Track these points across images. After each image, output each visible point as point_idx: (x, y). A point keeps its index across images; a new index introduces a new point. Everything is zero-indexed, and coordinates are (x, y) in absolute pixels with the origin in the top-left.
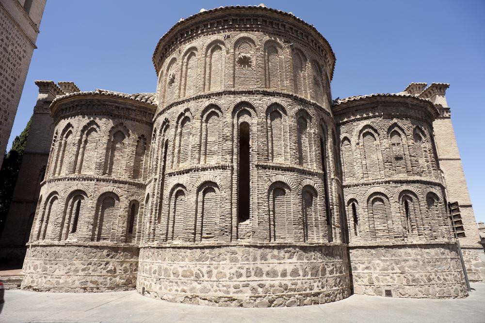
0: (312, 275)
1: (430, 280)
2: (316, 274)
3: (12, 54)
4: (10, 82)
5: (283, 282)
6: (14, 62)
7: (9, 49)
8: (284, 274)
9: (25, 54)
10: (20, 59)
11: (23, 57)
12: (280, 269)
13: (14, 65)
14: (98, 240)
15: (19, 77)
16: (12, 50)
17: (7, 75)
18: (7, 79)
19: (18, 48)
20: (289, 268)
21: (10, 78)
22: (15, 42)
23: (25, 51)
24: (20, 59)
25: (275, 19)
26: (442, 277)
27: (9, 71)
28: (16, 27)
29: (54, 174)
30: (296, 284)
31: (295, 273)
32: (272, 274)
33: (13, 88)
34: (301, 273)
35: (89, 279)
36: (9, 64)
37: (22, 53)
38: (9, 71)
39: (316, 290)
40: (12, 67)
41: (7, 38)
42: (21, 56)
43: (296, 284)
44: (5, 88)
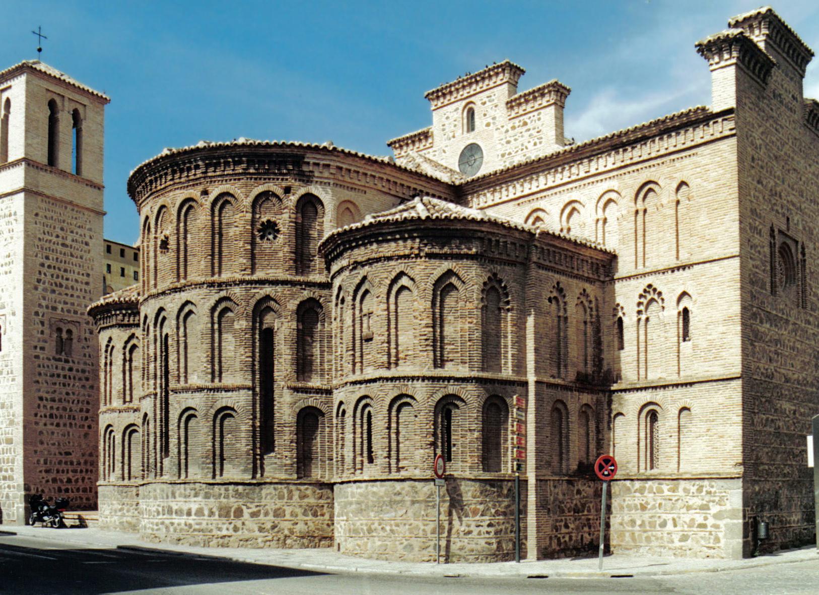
0: (220, 516)
2: (227, 515)
3: (74, 244)
6: (79, 253)
7: (69, 242)
9: (92, 233)
10: (87, 244)
11: (91, 238)
12: (185, 507)
13: (81, 258)
14: (399, 469)
15: (92, 269)
16: (73, 241)
17: (76, 276)
18: (76, 281)
19: (80, 231)
20: (194, 507)
21: (80, 278)
22: (73, 227)
23: (90, 230)
24: (87, 244)
27: (77, 269)
29: (106, 404)
31: (200, 512)
32: (179, 512)
33: (87, 288)
34: (206, 512)
35: (125, 519)
36: (74, 260)
37: (88, 233)
38: (77, 269)
39: (225, 532)
42: (87, 239)
43: (200, 524)
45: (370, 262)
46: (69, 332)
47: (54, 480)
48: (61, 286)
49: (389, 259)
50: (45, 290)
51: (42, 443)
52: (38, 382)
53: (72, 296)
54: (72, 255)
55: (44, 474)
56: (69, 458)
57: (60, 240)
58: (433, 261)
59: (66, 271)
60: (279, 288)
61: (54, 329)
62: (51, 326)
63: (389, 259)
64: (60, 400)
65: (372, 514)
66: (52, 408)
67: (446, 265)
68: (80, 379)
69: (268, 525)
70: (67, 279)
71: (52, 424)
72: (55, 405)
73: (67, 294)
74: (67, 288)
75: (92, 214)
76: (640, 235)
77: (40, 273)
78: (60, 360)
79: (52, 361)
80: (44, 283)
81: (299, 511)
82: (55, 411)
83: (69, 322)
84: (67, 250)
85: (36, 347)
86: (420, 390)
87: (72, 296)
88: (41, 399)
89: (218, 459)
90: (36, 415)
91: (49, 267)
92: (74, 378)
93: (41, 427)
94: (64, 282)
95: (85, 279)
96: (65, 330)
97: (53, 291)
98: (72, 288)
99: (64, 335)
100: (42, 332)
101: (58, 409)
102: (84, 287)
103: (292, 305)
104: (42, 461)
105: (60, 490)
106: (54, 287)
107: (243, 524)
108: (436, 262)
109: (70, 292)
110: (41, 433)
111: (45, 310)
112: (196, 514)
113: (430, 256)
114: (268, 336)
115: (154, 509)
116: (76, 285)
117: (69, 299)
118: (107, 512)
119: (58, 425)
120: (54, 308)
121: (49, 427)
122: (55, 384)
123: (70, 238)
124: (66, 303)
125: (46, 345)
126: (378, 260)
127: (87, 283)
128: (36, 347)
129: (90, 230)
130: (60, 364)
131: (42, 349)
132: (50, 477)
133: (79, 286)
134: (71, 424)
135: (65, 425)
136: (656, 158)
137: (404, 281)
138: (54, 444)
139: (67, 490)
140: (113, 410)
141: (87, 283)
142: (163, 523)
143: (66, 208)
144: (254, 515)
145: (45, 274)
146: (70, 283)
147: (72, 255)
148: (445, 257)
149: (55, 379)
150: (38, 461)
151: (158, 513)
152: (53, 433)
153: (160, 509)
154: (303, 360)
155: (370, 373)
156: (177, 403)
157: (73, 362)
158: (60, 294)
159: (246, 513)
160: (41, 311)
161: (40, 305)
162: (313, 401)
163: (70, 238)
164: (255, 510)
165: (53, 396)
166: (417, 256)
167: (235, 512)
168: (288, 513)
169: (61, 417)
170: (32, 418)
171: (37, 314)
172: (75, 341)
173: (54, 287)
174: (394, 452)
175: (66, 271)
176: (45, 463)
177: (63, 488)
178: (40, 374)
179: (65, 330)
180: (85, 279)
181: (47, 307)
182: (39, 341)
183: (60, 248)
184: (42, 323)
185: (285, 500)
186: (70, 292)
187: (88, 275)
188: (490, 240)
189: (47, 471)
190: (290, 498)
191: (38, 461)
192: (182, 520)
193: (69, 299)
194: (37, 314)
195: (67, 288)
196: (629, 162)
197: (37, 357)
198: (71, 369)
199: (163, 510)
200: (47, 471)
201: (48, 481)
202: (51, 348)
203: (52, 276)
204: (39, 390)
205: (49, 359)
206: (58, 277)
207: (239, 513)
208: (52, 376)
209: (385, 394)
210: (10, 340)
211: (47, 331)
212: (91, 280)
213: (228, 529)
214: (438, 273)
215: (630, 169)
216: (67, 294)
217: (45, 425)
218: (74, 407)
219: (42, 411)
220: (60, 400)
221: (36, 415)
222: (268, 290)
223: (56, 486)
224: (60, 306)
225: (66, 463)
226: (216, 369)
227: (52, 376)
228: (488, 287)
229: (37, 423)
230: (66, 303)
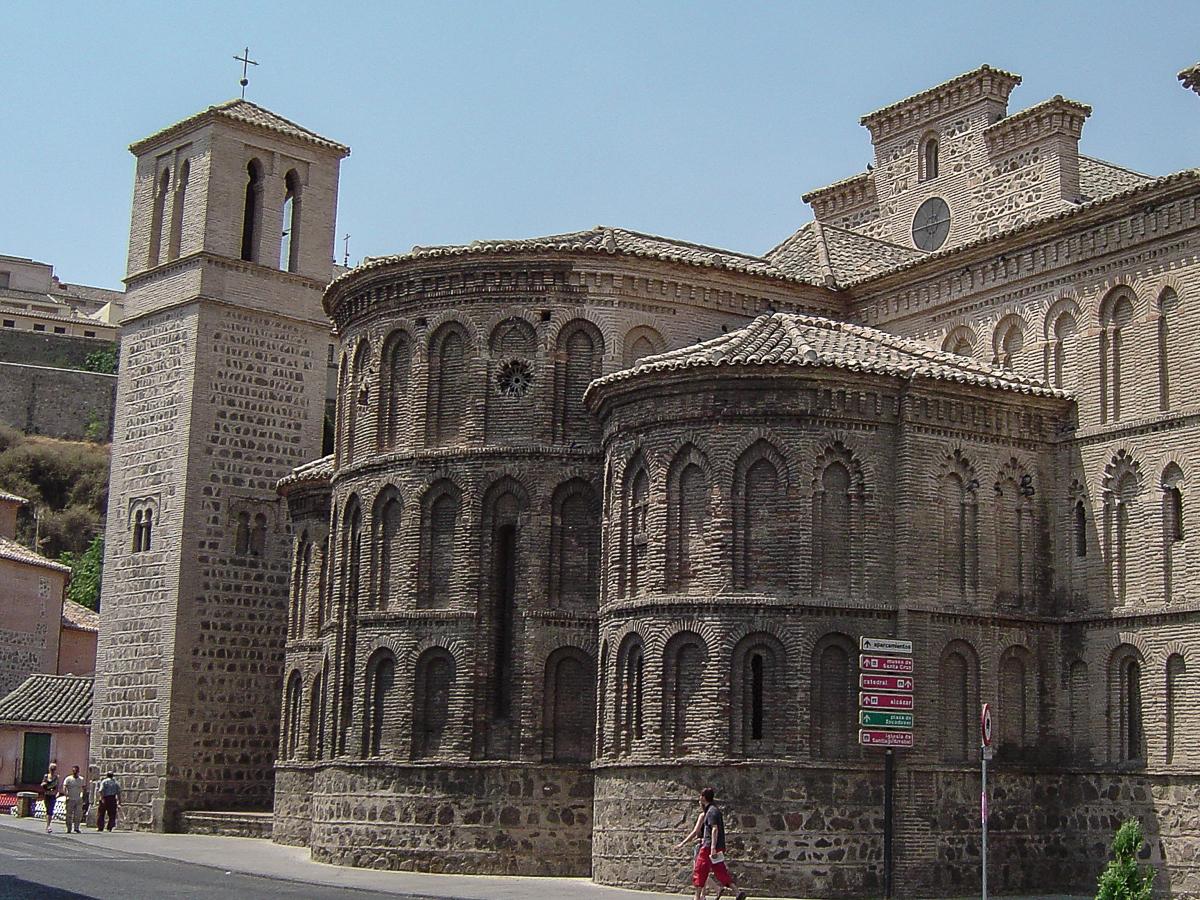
0: (418, 820)
1: (632, 848)
2: (429, 819)
4: (287, 439)
5: (372, 828)
6: (284, 393)
7: (268, 376)
8: (373, 816)
10: (299, 377)
11: (306, 367)
12: (368, 805)
16: (275, 373)
17: (277, 429)
18: (278, 437)
19: (288, 357)
20: (381, 805)
21: (284, 432)
23: (306, 354)
24: (299, 377)
25: (394, 278)
26: (656, 844)
27: (279, 418)
28: (273, 320)
30: (388, 833)
31: (388, 814)
34: (398, 814)
37: (302, 360)
38: (279, 418)
39: (422, 847)
40: (284, 405)
41: (259, 356)
42: (300, 369)
43: (388, 833)
44: (279, 455)
45: (646, 427)
46: (261, 517)
47: (219, 758)
48: (252, 445)
49: (671, 423)
50: (224, 453)
51: (202, 697)
52: (202, 599)
53: (269, 460)
54: (273, 397)
55: (201, 748)
56: (248, 721)
57: (255, 375)
58: (735, 427)
59: (260, 422)
60: (526, 465)
61: (236, 514)
62: (230, 510)
63: (671, 423)
64: (238, 628)
65: (635, 822)
66: (223, 640)
67: (755, 432)
68: (274, 593)
69: (492, 837)
70: (263, 435)
71: (221, 666)
72: (229, 635)
73: (260, 459)
74: (261, 448)
75: (311, 329)
76: (1110, 373)
77: (217, 427)
78: (242, 563)
79: (229, 566)
80: (223, 443)
81: (543, 816)
82: (227, 646)
83: (261, 502)
84: (266, 389)
85: (202, 544)
86: (710, 630)
87: (269, 460)
88: (206, 625)
89: (425, 729)
90: (196, 652)
91: (234, 417)
92: (265, 591)
93: (203, 671)
94: (257, 441)
95: (293, 432)
96: (253, 515)
97: (238, 455)
98: (270, 448)
99: (252, 523)
100: (215, 520)
101: (233, 641)
102: (290, 445)
103: (545, 490)
104: (200, 727)
105: (227, 775)
106: (239, 448)
107: (453, 834)
108: (738, 428)
109: (266, 454)
110: (202, 680)
111: (221, 485)
112: (382, 817)
113: (731, 419)
114: (507, 536)
115: (327, 807)
116: (276, 443)
117: (264, 466)
118: (283, 813)
119: (231, 668)
120: (238, 482)
121: (217, 671)
122: (231, 601)
123: (270, 370)
124: (257, 472)
125: (221, 540)
126: (655, 425)
127: (296, 440)
128: (202, 544)
129: (306, 354)
130: (242, 570)
131: (213, 546)
132: (212, 753)
133: (281, 444)
134: (254, 667)
135: (244, 668)
136: (1131, 248)
137: (694, 458)
138: (222, 699)
139: (240, 776)
140: (302, 648)
141: (296, 440)
142: (336, 831)
143: (267, 323)
144: (471, 818)
145: (225, 428)
146: (266, 441)
147: (273, 397)
148: (754, 419)
149: (230, 595)
150: (194, 727)
151: (332, 816)
152: (222, 681)
153: (334, 807)
154: (560, 573)
155: (644, 597)
156: (369, 641)
157: (265, 566)
158: (249, 459)
159: (458, 815)
160: (215, 487)
161: (214, 478)
162: (573, 637)
163: (270, 370)
164: (471, 810)
165: (225, 621)
166: (712, 420)
167: (440, 815)
168: (523, 818)
169: (238, 655)
170: (189, 657)
171: (208, 491)
172: (270, 531)
173: (239, 448)
174: (673, 728)
175: (260, 422)
176: (206, 729)
177: (234, 771)
178: (207, 586)
179: (253, 515)
180: (293, 432)
181: (226, 480)
182: (209, 534)
183: (253, 386)
184: (217, 506)
185: (521, 796)
186: (266, 454)
187: (298, 427)
188: (828, 393)
189: (207, 744)
190: (529, 791)
191: (194, 727)
192: (361, 826)
193: (264, 466)
194: (208, 491)
195: (261, 448)
196: (1089, 255)
197: (204, 559)
198: (259, 578)
199: (338, 809)
200: (207, 744)
201: (207, 760)
202: (227, 547)
203: (238, 431)
204: (204, 612)
205: (223, 562)
206: (247, 432)
207: (447, 816)
208: (228, 588)
209: (657, 635)
210: (163, 533)
211: (223, 517)
212: (302, 433)
213: (428, 842)
214: (746, 442)
215: (1092, 266)
216: (260, 459)
217: (210, 667)
218: (262, 639)
219: (207, 646)
220: (238, 628)
221: (196, 652)
222: (509, 467)
223: (222, 767)
224: (248, 478)
225: (241, 730)
226: (430, 585)
227: (228, 588)
228: (827, 463)
229: (196, 665)
230: (257, 472)
